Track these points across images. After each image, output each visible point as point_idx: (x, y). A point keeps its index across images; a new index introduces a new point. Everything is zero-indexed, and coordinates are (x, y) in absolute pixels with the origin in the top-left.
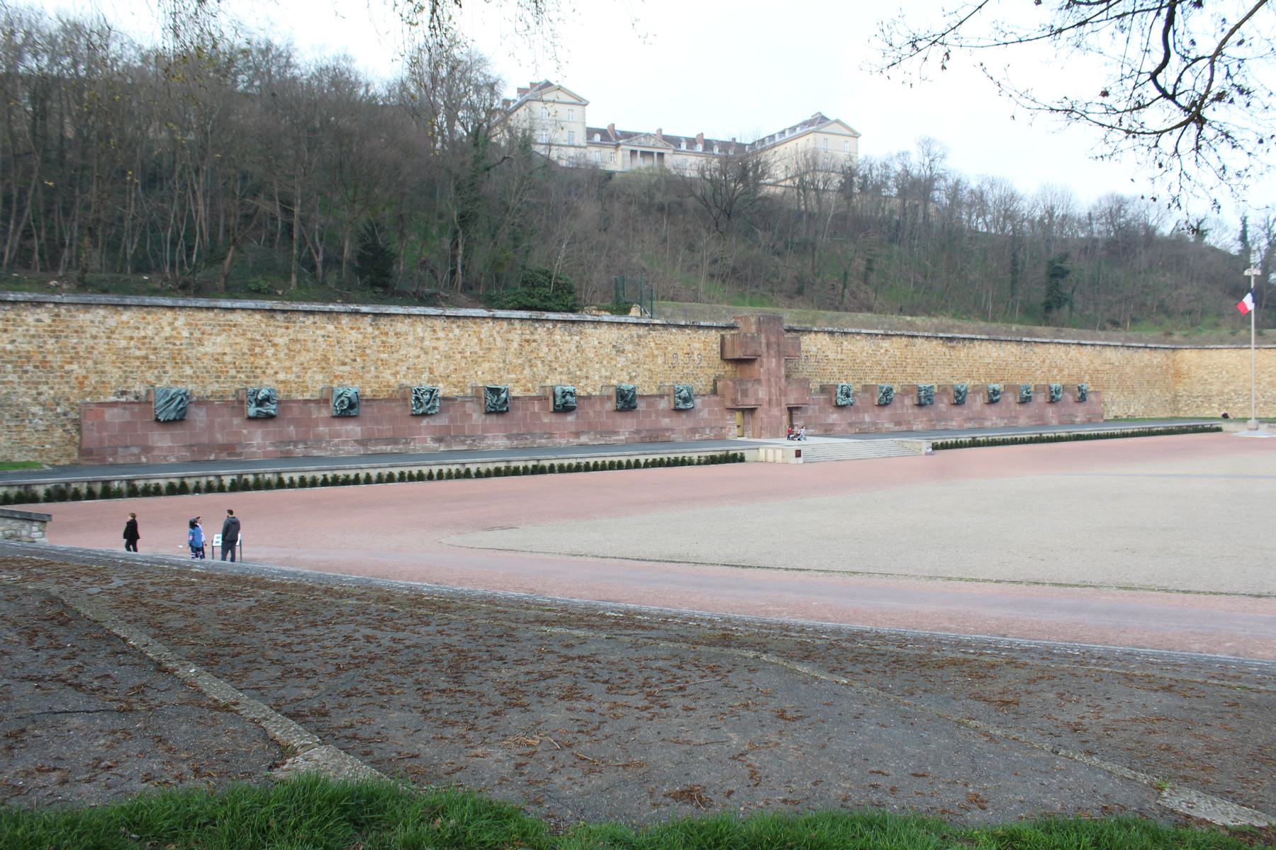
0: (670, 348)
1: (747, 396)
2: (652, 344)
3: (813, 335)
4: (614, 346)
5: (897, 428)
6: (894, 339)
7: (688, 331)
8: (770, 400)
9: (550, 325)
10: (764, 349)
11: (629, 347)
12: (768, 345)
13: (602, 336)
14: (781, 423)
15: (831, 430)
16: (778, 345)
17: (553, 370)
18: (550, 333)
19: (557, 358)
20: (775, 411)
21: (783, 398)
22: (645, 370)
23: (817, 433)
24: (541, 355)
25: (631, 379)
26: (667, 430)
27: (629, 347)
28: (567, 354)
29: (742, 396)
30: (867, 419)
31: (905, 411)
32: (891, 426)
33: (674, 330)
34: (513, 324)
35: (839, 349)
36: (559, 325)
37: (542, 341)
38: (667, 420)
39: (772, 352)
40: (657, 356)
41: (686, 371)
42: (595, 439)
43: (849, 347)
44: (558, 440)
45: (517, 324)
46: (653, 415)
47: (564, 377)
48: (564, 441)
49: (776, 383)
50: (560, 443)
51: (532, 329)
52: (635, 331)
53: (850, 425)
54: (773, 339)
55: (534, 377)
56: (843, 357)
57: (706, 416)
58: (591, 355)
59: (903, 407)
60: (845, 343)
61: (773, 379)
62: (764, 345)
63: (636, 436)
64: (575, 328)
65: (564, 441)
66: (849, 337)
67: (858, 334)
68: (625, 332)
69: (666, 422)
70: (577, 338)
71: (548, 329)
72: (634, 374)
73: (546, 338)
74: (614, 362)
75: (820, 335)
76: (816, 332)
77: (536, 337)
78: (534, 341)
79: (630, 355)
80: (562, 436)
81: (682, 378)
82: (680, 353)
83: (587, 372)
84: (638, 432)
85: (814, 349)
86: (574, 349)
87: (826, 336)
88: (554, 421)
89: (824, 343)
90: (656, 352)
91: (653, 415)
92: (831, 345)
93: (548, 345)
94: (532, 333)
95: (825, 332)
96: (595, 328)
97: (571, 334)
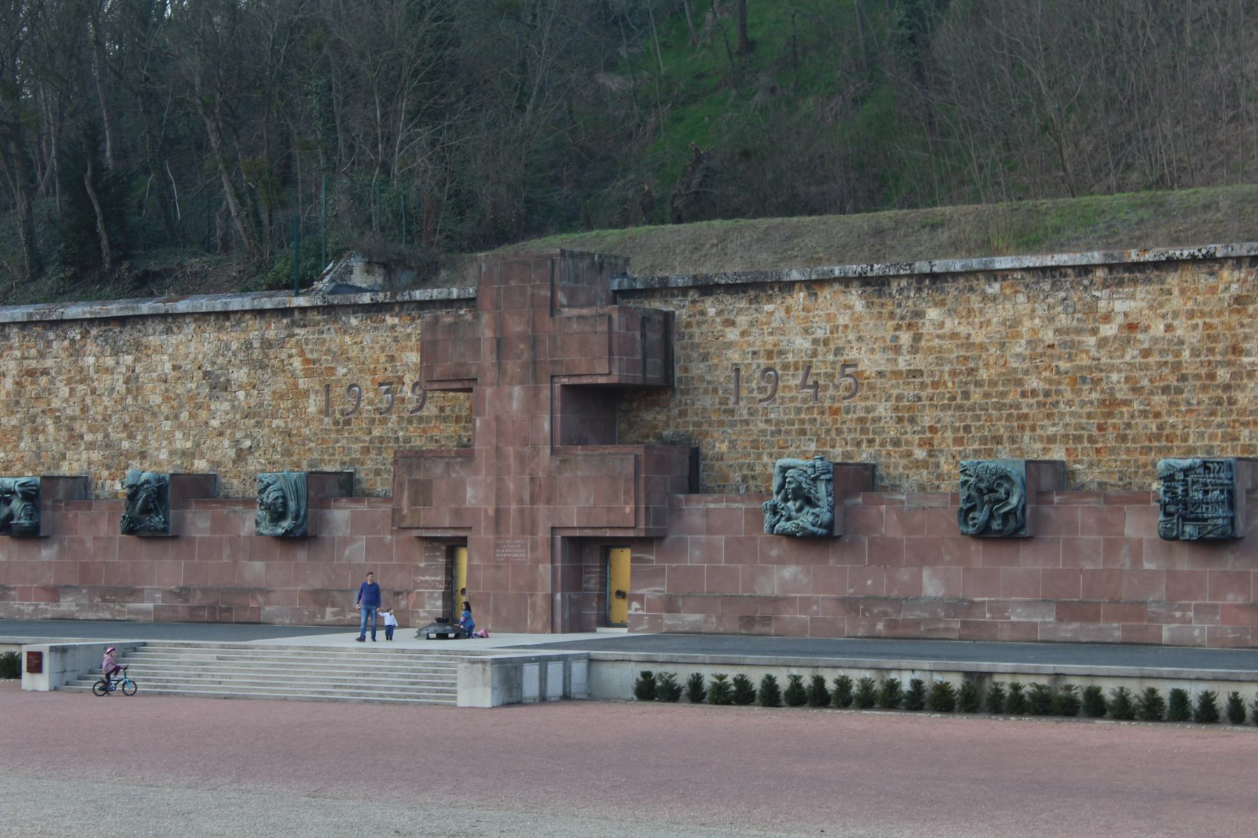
0: (341, 371)
1: (427, 502)
2: (297, 363)
3: (801, 296)
4: (206, 374)
5: (1069, 630)
6: (1173, 279)
7: (390, 320)
8: (498, 520)
9: (75, 333)
10: (488, 357)
11: (240, 375)
12: (501, 345)
13: (182, 350)
14: (532, 587)
15: (766, 620)
16: (534, 343)
17: (74, 438)
18: (76, 351)
19: (85, 410)
20: (516, 551)
21: (541, 507)
22: (274, 431)
23: (712, 624)
24: (56, 403)
25: (241, 455)
26: (251, 592)
27: (240, 375)
28: (106, 401)
29: (414, 502)
30: (932, 586)
31: (1125, 562)
32: (1045, 619)
33: (354, 321)
34: (7, 338)
35: (905, 338)
36: (94, 332)
37: (59, 373)
38: (259, 566)
39: (513, 367)
40: (306, 394)
41: (377, 432)
42: (92, 607)
43: (950, 324)
44: (16, 605)
45: (15, 335)
46: (227, 551)
47: (96, 456)
48: (28, 608)
49: (521, 458)
50: (20, 611)
51: (41, 344)
52: (255, 331)
53: (850, 605)
54: (517, 326)
55: (38, 455)
56: (919, 362)
57: (361, 558)
58: (156, 400)
59: (1112, 547)
60: (933, 314)
61: (510, 450)
62: (486, 347)
63: (179, 604)
64: (126, 336)
65: (28, 608)
66: (951, 288)
67: (993, 275)
68: (234, 338)
69: (255, 570)
70: (129, 359)
71: (73, 341)
72: (248, 443)
73: (66, 363)
74: (203, 414)
75: (826, 293)
76: (812, 286)
77: (49, 363)
78: (45, 372)
79: (241, 395)
80: (24, 597)
81: (366, 450)
82: (366, 382)
83: (144, 442)
84: (183, 593)
85: (802, 343)
86: (121, 387)
87: (855, 299)
88: (15, 559)
89: (843, 320)
90: (303, 384)
91: (227, 551)
92: (869, 326)
93: (69, 381)
94: (42, 355)
95: (846, 281)
96: (169, 331)
97: (116, 353)
